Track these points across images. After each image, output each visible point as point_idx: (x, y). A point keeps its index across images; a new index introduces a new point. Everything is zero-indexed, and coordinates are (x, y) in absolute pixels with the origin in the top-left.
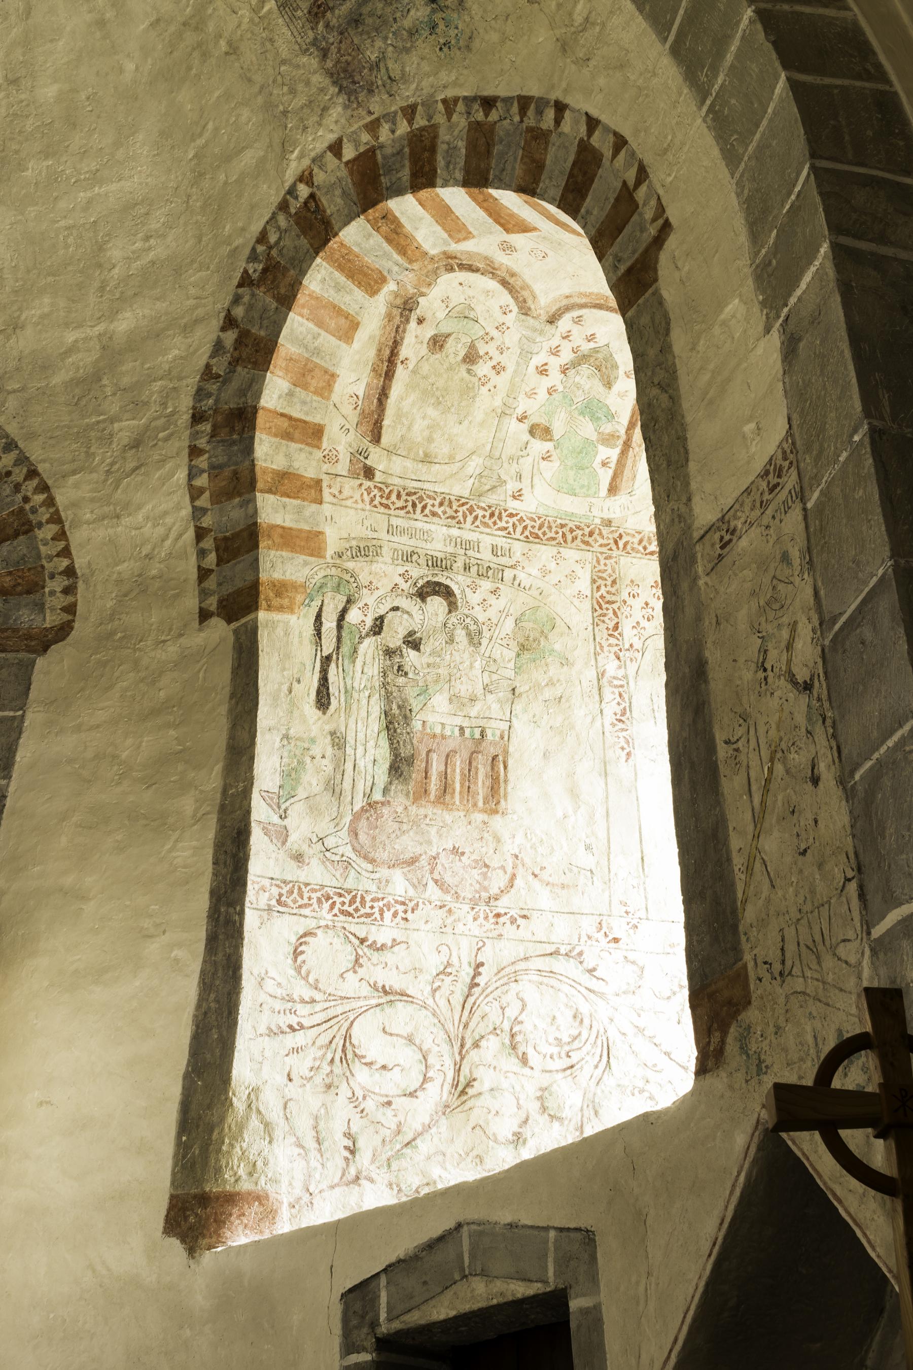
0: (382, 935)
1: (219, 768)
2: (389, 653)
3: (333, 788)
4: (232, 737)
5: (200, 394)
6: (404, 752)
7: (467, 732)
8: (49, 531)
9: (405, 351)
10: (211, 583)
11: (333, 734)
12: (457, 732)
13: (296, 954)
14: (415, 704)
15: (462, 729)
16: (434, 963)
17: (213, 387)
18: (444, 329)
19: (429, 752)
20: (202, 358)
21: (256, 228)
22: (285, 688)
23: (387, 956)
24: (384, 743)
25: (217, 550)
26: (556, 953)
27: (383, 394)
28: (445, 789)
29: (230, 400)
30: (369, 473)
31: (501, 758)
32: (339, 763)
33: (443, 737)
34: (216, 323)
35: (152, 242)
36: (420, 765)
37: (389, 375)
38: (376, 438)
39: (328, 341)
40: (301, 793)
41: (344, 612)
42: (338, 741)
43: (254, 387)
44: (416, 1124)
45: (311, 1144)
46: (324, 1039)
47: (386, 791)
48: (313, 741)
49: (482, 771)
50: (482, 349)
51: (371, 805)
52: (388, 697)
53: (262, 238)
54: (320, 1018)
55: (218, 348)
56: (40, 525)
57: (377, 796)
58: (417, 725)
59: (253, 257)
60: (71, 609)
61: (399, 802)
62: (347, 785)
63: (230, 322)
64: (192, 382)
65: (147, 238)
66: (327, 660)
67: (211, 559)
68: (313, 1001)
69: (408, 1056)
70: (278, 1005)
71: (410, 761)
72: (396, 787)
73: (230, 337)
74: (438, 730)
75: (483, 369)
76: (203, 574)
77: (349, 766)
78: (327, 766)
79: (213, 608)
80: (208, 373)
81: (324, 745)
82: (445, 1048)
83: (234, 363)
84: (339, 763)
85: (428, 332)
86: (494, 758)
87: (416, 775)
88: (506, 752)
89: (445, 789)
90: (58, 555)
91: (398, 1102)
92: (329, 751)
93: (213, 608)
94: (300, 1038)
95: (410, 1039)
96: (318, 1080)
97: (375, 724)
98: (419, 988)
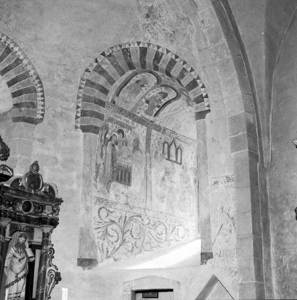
0: (111, 210)
2: (113, 145)
8: (40, 94)
10: (79, 120)
13: (99, 213)
16: (119, 215)
23: (113, 214)
25: (81, 112)
26: (137, 216)
30: (114, 103)
38: (118, 95)
41: (106, 134)
44: (117, 247)
45: (101, 250)
46: (103, 230)
50: (145, 85)
54: (102, 226)
55: (91, 65)
56: (38, 92)
60: (43, 115)
66: (103, 146)
67: (79, 115)
68: (101, 223)
69: (116, 234)
70: (96, 223)
73: (95, 64)
76: (77, 117)
79: (79, 126)
82: (121, 233)
90: (41, 101)
91: (114, 243)
93: (79, 126)
94: (100, 230)
95: (115, 231)
96: (103, 238)
98: (117, 221)
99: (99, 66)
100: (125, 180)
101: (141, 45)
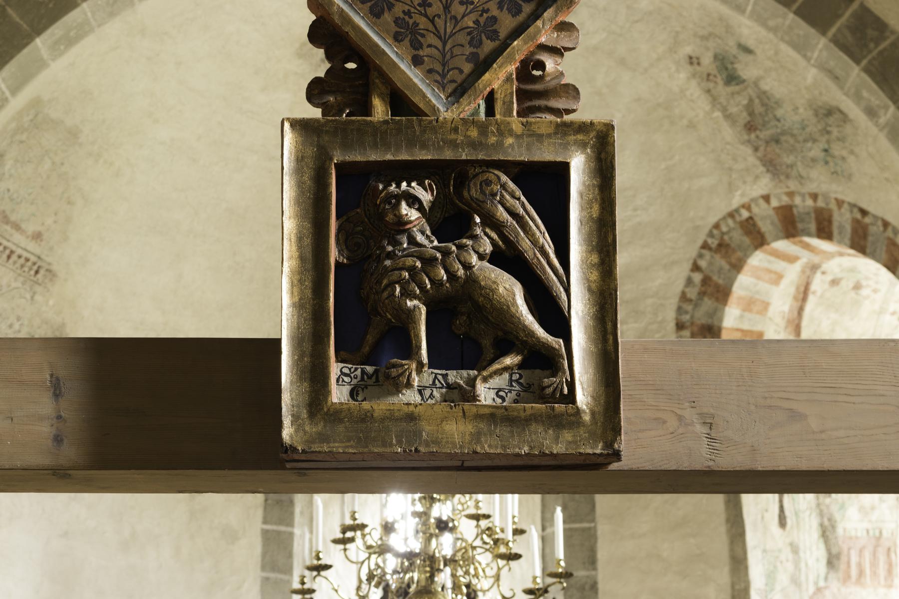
1: (726, 570)
3: (795, 581)
4: (732, 550)
5: (680, 310)
6: (834, 551)
7: (871, 533)
9: (814, 287)
11: (791, 544)
12: (865, 533)
14: (837, 516)
15: (868, 531)
17: (689, 308)
18: (839, 275)
19: (849, 549)
20: (679, 286)
21: (713, 220)
22: (759, 517)
24: (822, 546)
27: (801, 310)
28: (861, 573)
29: (701, 316)
31: (892, 549)
32: (797, 564)
33: (857, 538)
34: (688, 266)
35: (639, 212)
36: (844, 558)
37: (804, 299)
39: (763, 286)
40: (778, 587)
42: (795, 549)
43: (717, 313)
47: (826, 579)
48: (780, 551)
49: (882, 558)
50: (864, 283)
51: (819, 590)
52: (821, 514)
53: (717, 226)
55: (689, 282)
57: (822, 583)
58: (840, 531)
59: (711, 235)
61: (834, 585)
62: (803, 578)
63: (696, 268)
64: (673, 302)
65: (635, 210)
71: (838, 556)
72: (832, 575)
73: (697, 277)
74: (853, 533)
75: (865, 292)
77: (803, 565)
78: (790, 566)
80: (684, 297)
81: (787, 554)
83: (702, 294)
84: (797, 564)
85: (829, 278)
86: (889, 549)
87: (843, 566)
88: (895, 545)
89: (861, 573)
92: (790, 556)
97: (815, 533)
99: (706, 281)
100: (875, 574)
101: (775, 203)
